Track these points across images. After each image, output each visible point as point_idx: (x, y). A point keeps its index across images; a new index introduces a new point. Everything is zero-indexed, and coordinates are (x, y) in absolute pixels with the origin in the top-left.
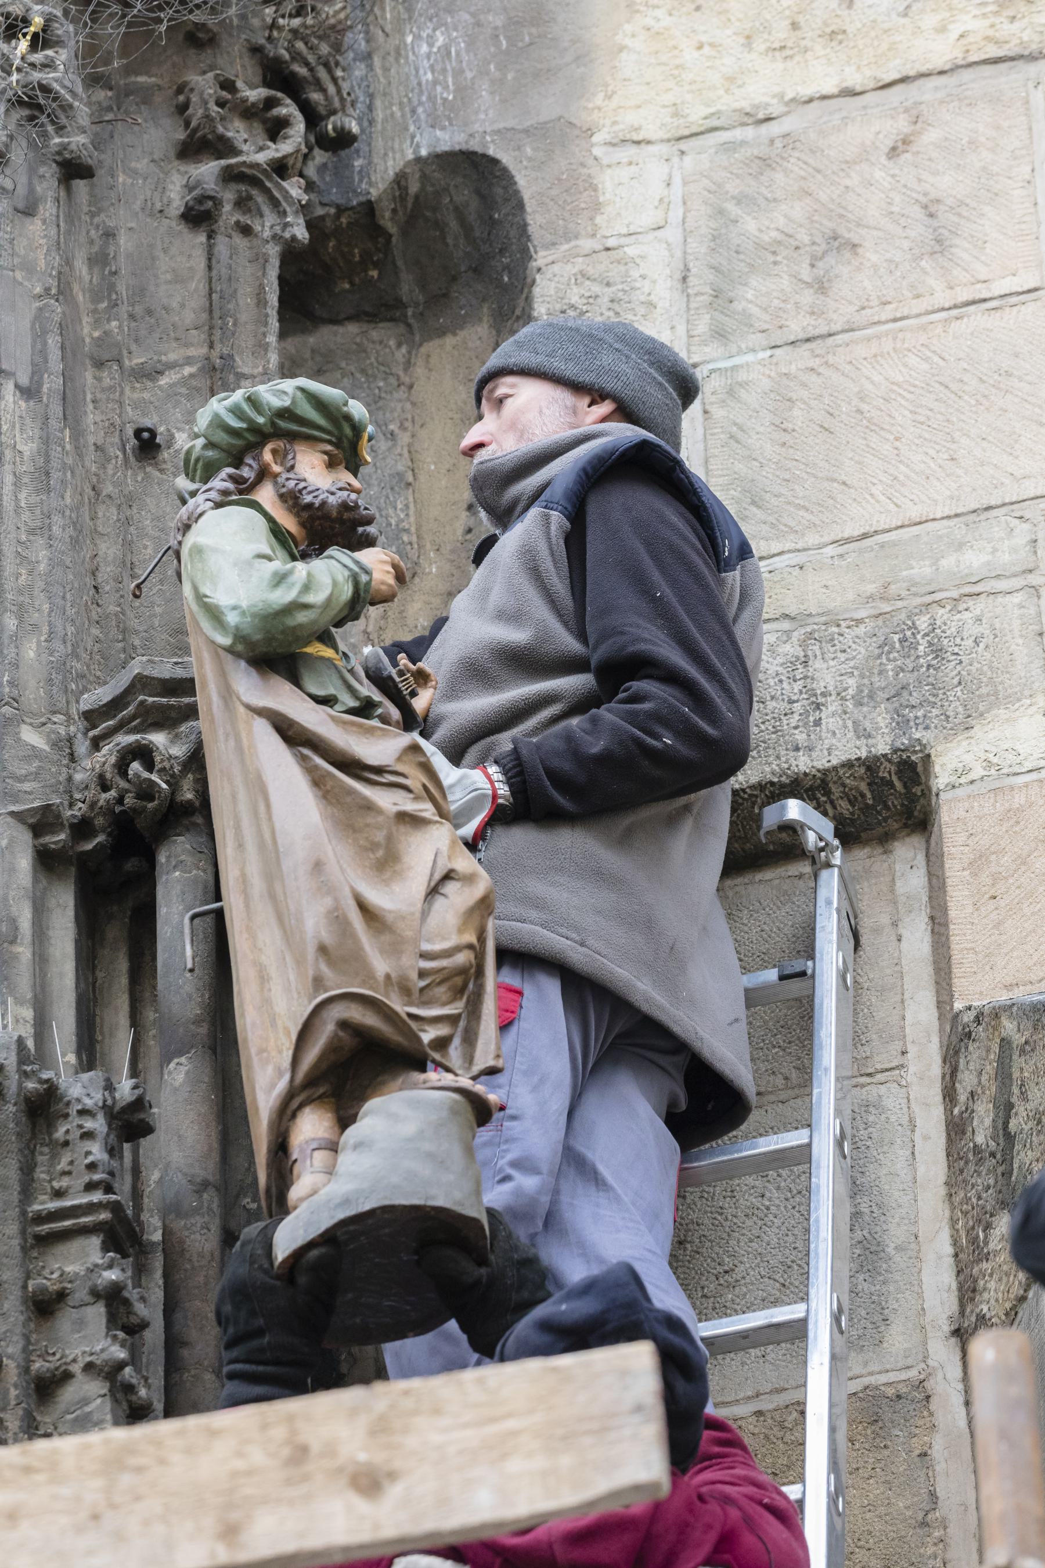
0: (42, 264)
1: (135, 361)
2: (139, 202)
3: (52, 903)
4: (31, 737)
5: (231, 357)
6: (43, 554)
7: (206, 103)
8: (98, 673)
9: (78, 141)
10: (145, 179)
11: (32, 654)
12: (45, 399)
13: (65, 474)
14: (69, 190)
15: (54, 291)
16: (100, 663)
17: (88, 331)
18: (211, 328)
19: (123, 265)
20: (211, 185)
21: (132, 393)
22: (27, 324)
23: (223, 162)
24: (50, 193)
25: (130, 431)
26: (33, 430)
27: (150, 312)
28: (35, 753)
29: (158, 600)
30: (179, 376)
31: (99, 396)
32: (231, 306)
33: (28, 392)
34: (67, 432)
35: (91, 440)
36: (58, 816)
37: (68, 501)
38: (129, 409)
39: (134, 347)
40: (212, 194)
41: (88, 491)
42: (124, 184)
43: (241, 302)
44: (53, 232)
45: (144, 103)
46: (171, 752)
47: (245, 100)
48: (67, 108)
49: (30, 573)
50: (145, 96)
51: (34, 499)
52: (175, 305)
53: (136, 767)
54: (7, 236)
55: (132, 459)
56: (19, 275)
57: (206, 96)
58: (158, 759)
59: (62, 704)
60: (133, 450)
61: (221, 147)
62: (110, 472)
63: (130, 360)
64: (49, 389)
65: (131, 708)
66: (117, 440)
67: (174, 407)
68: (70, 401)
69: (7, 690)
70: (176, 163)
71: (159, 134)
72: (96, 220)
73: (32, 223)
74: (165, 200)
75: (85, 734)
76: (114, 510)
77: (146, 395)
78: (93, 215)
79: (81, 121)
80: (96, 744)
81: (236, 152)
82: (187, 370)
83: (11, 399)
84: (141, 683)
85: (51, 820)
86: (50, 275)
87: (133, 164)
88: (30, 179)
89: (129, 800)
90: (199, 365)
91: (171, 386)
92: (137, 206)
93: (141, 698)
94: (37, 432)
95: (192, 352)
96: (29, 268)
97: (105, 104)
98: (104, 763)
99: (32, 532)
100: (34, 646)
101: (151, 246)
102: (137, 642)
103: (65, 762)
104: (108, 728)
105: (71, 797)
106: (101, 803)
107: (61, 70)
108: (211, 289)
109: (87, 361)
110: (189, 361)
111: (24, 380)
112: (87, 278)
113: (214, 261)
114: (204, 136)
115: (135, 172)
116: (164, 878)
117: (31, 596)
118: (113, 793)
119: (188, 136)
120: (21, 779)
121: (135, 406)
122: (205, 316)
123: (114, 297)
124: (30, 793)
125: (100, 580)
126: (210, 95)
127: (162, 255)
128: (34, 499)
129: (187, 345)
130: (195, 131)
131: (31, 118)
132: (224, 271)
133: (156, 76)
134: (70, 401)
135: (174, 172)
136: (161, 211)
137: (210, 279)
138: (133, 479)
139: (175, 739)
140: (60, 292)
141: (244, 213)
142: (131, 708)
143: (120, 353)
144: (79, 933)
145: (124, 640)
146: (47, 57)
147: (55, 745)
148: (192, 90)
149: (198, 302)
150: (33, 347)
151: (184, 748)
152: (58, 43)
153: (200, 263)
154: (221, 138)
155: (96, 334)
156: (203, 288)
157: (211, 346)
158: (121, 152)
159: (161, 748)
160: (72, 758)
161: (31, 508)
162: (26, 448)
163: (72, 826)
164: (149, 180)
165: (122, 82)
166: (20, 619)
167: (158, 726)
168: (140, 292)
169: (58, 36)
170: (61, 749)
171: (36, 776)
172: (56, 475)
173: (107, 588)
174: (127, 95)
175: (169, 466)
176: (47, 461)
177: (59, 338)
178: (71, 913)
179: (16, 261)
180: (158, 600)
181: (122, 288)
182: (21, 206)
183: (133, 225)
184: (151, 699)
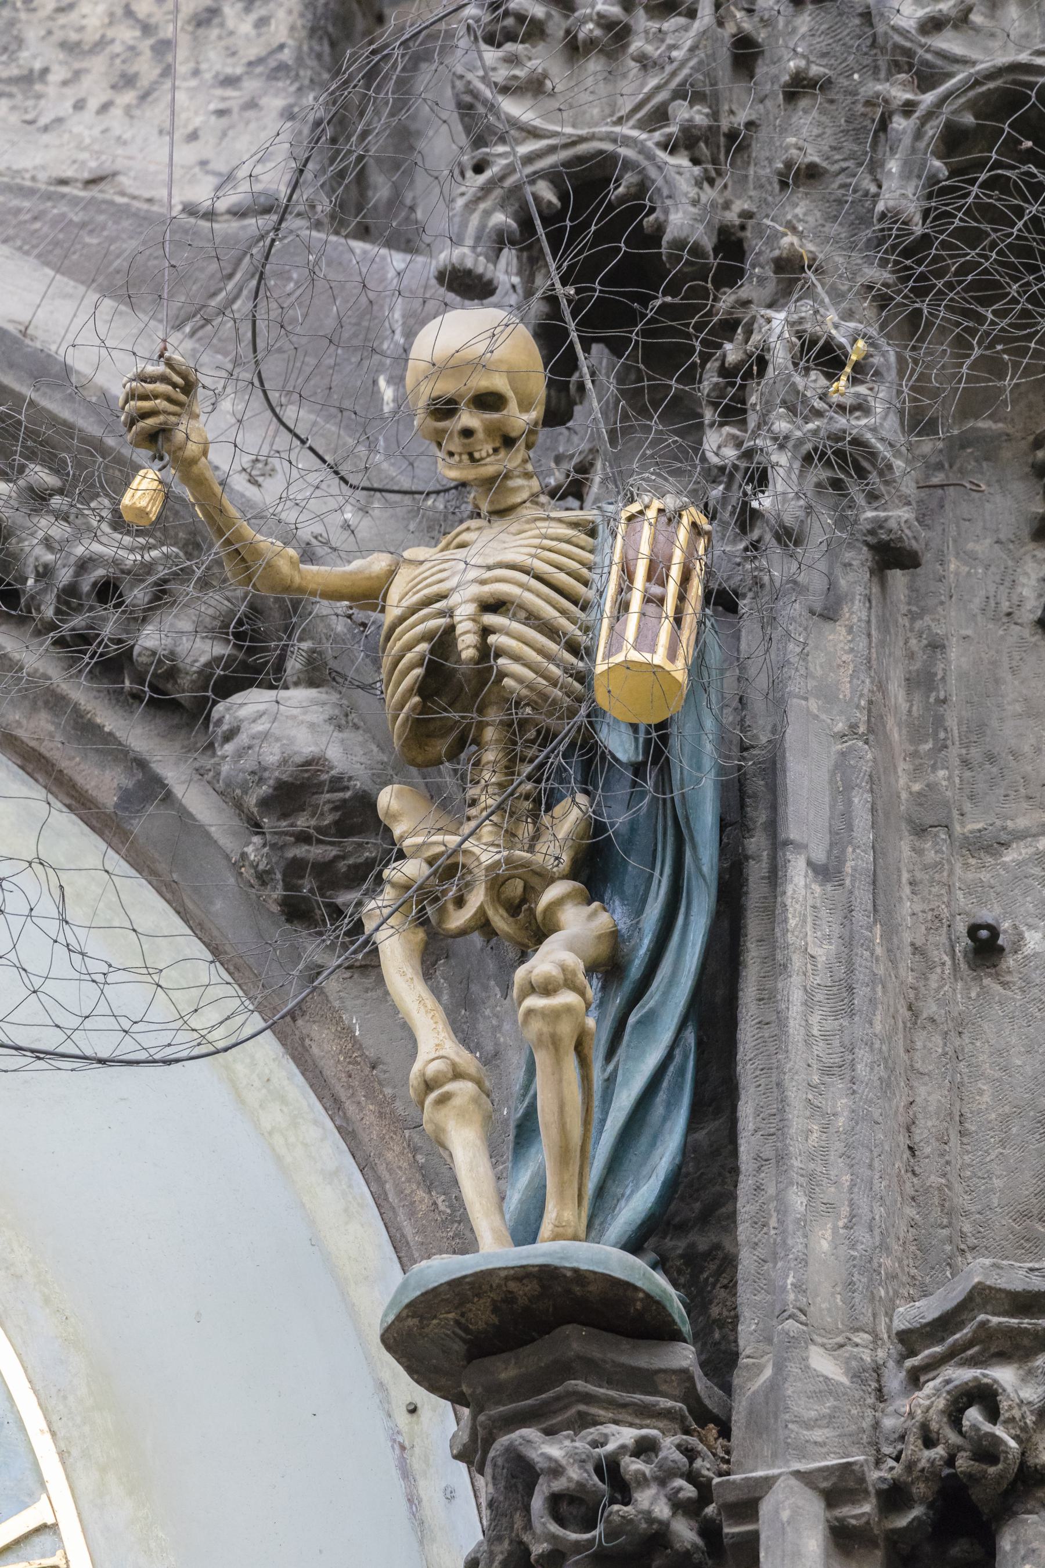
0: (846, 688)
4: (823, 1363)
8: (913, 1271)
10: (987, 567)
11: (825, 1245)
14: (883, 584)
15: (862, 729)
19: (953, 688)
25: (961, 928)
27: (991, 758)
28: (829, 1388)
29: (998, 1169)
31: (919, 875)
35: (907, 937)
36: (862, 1480)
38: (960, 894)
39: (967, 807)
44: (862, 644)
49: (824, 1129)
50: (987, 448)
51: (831, 1024)
52: (1026, 748)
53: (973, 1415)
55: (963, 966)
56: (813, 705)
58: (1004, 1405)
63: (963, 824)
65: (966, 1332)
66: (943, 939)
67: (1025, 894)
69: (792, 1296)
70: (1031, 546)
72: (918, 624)
76: (938, 1039)
78: (913, 617)
80: (915, 1379)
84: (980, 1297)
85: (852, 1484)
87: (970, 546)
89: (963, 1463)
91: (1020, 864)
93: (982, 1317)
94: (837, 929)
96: (828, 695)
99: (827, 1071)
100: (828, 1234)
101: (994, 663)
102: (967, 1228)
103: (870, 1401)
109: (904, 826)
111: (819, 855)
112: (904, 706)
115: (971, 558)
117: (826, 1163)
118: (939, 1451)
120: (808, 1425)
121: (969, 892)
124: (823, 1444)
127: (1009, 677)
135: (1028, 558)
140: (870, 730)
142: (966, 1332)
143: (949, 816)
147: (857, 1376)
150: (832, 807)
155: (916, 787)
160: (880, 1395)
161: (826, 1037)
163: (879, 1493)
166: (811, 1196)
167: (1003, 1357)
168: (977, 729)
170: (864, 1382)
171: (829, 1420)
172: (862, 992)
173: (928, 1150)
176: (851, 971)
177: (868, 796)
180: (998, 1169)
181: (951, 722)
183: (969, 632)
184: (995, 1320)
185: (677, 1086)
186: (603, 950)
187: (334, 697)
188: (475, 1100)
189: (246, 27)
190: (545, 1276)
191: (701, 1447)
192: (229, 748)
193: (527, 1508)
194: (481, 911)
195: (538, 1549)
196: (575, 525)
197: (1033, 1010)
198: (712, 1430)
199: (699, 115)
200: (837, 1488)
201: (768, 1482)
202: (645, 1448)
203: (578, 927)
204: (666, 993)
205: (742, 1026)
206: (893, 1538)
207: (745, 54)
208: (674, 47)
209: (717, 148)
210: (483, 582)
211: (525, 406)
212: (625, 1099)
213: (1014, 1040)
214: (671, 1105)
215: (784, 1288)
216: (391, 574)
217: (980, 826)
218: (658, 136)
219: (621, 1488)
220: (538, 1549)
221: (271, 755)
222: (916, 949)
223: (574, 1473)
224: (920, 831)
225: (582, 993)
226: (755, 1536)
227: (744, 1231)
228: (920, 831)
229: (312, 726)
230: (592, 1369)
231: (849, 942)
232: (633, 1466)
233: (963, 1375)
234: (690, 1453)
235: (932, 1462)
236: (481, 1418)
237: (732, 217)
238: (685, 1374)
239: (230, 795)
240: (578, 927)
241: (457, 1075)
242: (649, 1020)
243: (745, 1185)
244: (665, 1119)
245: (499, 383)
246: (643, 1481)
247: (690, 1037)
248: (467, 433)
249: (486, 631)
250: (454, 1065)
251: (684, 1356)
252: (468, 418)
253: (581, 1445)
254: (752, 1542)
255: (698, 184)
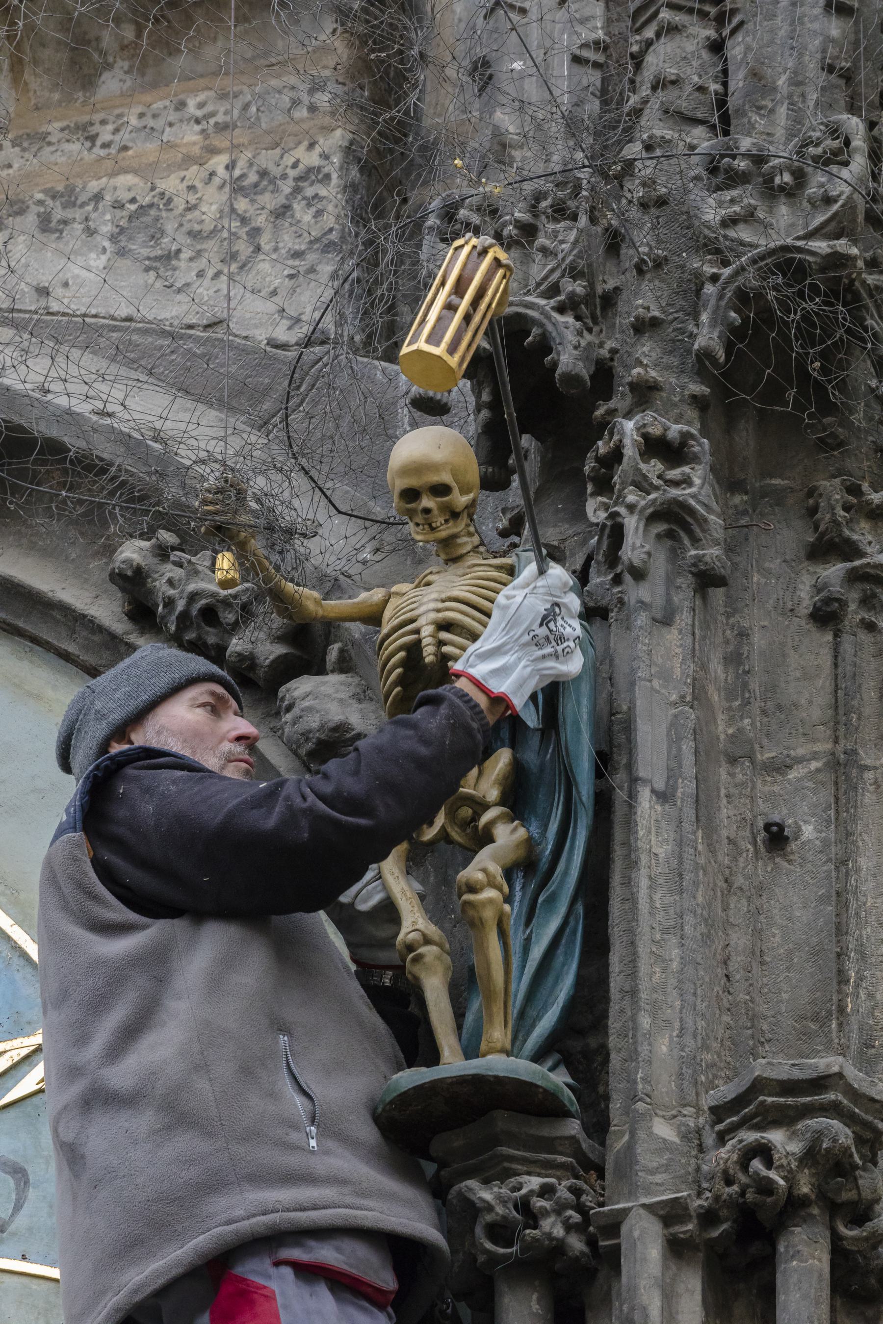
0: (678, 672)
1: (767, 755)
2: (771, 601)
3: (681, 1288)
4: (664, 1130)
5: (855, 752)
6: (675, 952)
7: (833, 509)
8: (729, 1059)
9: (712, 553)
10: (778, 578)
11: (664, 1049)
12: (679, 803)
13: (697, 875)
14: (704, 598)
15: (688, 698)
16: (730, 1050)
17: (722, 728)
18: (837, 723)
19: (756, 664)
20: (836, 589)
21: (763, 787)
22: (663, 730)
23: (848, 565)
24: (687, 603)
25: (761, 824)
26: (668, 833)
27: (780, 708)
30: (806, 770)
31: (732, 791)
32: (855, 703)
33: (663, 797)
34: (700, 833)
35: (724, 833)
37: (700, 899)
39: (765, 742)
40: (838, 596)
41: (721, 884)
42: (758, 584)
43: (865, 697)
44: (689, 640)
45: (777, 505)
46: (788, 1148)
47: (869, 503)
48: (703, 522)
49: (664, 970)
50: (778, 497)
51: (669, 899)
52: (803, 701)
54: (645, 648)
55: (762, 849)
57: (833, 502)
58: (776, 1156)
59: (691, 1097)
60: (764, 842)
61: (848, 550)
62: (742, 865)
63: (762, 753)
64: (683, 794)
66: (748, 834)
67: (802, 800)
68: (703, 805)
70: (806, 563)
71: (789, 536)
72: (732, 620)
73: (670, 632)
74: (796, 599)
75: (712, 1127)
76: (744, 902)
77: (776, 788)
78: (728, 616)
79: (715, 534)
80: (722, 1139)
81: (861, 554)
82: (814, 765)
83: (648, 806)
84: (758, 1086)
86: (685, 683)
87: (767, 565)
88: (668, 589)
89: (750, 1196)
90: (824, 760)
91: (799, 780)
92: (770, 605)
93: (761, 1098)
94: (672, 835)
95: (819, 747)
96: (665, 675)
97: (741, 508)
98: (727, 1160)
99: (666, 931)
100: (666, 1041)
102: (765, 1027)
103: (694, 1153)
104: (732, 1123)
105: (699, 1186)
106: (725, 1196)
107: (697, 485)
108: (836, 686)
109: (722, 758)
110: (815, 756)
112: (723, 677)
113: (840, 659)
114: (832, 539)
115: (769, 571)
116: (783, 1266)
117: (665, 993)
119: (817, 539)
120: (653, 1172)
121: (766, 800)
122: (830, 712)
123: (747, 695)
125: (731, 969)
126: (836, 500)
128: (669, 899)
129: (814, 741)
130: (823, 535)
131: (670, 535)
132: (848, 668)
133: (789, 478)
134: (703, 805)
135: (804, 572)
136: (792, 610)
137: (836, 676)
138: (763, 870)
139: (793, 1136)
140: (694, 698)
141: (869, 610)
143: (753, 751)
144: (707, 1315)
145: (752, 1027)
146: (683, 474)
147: (684, 1137)
148: (821, 495)
149: (823, 699)
150: (669, 752)
151: (800, 1145)
152: (694, 459)
153: (826, 660)
154: (848, 541)
155: (730, 731)
156: (829, 687)
157: (836, 741)
158: (756, 552)
159: (779, 1146)
160: (701, 1148)
161: (665, 909)
162: (661, 850)
164: (781, 580)
165: (757, 485)
166: (654, 1016)
167: (776, 1123)
168: (771, 689)
169: (695, 454)
171: (666, 1168)
172: (688, 876)
173: (738, 977)
174: (762, 497)
175: (795, 857)
176: (681, 863)
177: (692, 744)
178: (698, 1297)
179: (654, 670)
181: (754, 685)
182: (659, 616)
183: (766, 623)
184: (770, 1099)
185: (573, 942)
186: (522, 852)
187: (357, 679)
188: (438, 958)
189: (307, 218)
190: (477, 1081)
191: (585, 1187)
192: (289, 717)
193: (472, 1231)
194: (443, 828)
195: (481, 1258)
196: (499, 568)
197: (808, 878)
198: (593, 1175)
199: (578, 287)
200: (670, 1214)
201: (626, 1212)
202: (546, 1191)
203: (508, 836)
204: (562, 882)
205: (611, 902)
206: (711, 1244)
207: (614, 243)
208: (562, 242)
209: (595, 308)
210: (438, 611)
211: (464, 491)
212: (537, 952)
213: (795, 899)
214: (568, 955)
215: (635, 1082)
216: (386, 602)
217: (773, 755)
218: (553, 302)
219: (532, 1217)
220: (481, 1258)
221: (313, 722)
222: (730, 841)
223: (500, 1210)
224: (733, 760)
225: (500, 889)
226: (618, 1247)
227: (613, 1041)
228: (733, 760)
229: (341, 701)
230: (513, 1140)
231: (680, 843)
232: (539, 1203)
233: (750, 1136)
234: (576, 1191)
235: (730, 1196)
236: (442, 1173)
237: (604, 352)
238: (573, 1139)
239: (293, 748)
240: (508, 836)
241: (427, 941)
242: (552, 899)
243: (614, 1009)
244: (564, 965)
245: (446, 478)
246: (545, 1213)
247: (580, 908)
248: (427, 511)
249: (441, 643)
250: (424, 935)
251: (573, 1127)
252: (427, 502)
253: (504, 1191)
254: (616, 1251)
255: (580, 334)
